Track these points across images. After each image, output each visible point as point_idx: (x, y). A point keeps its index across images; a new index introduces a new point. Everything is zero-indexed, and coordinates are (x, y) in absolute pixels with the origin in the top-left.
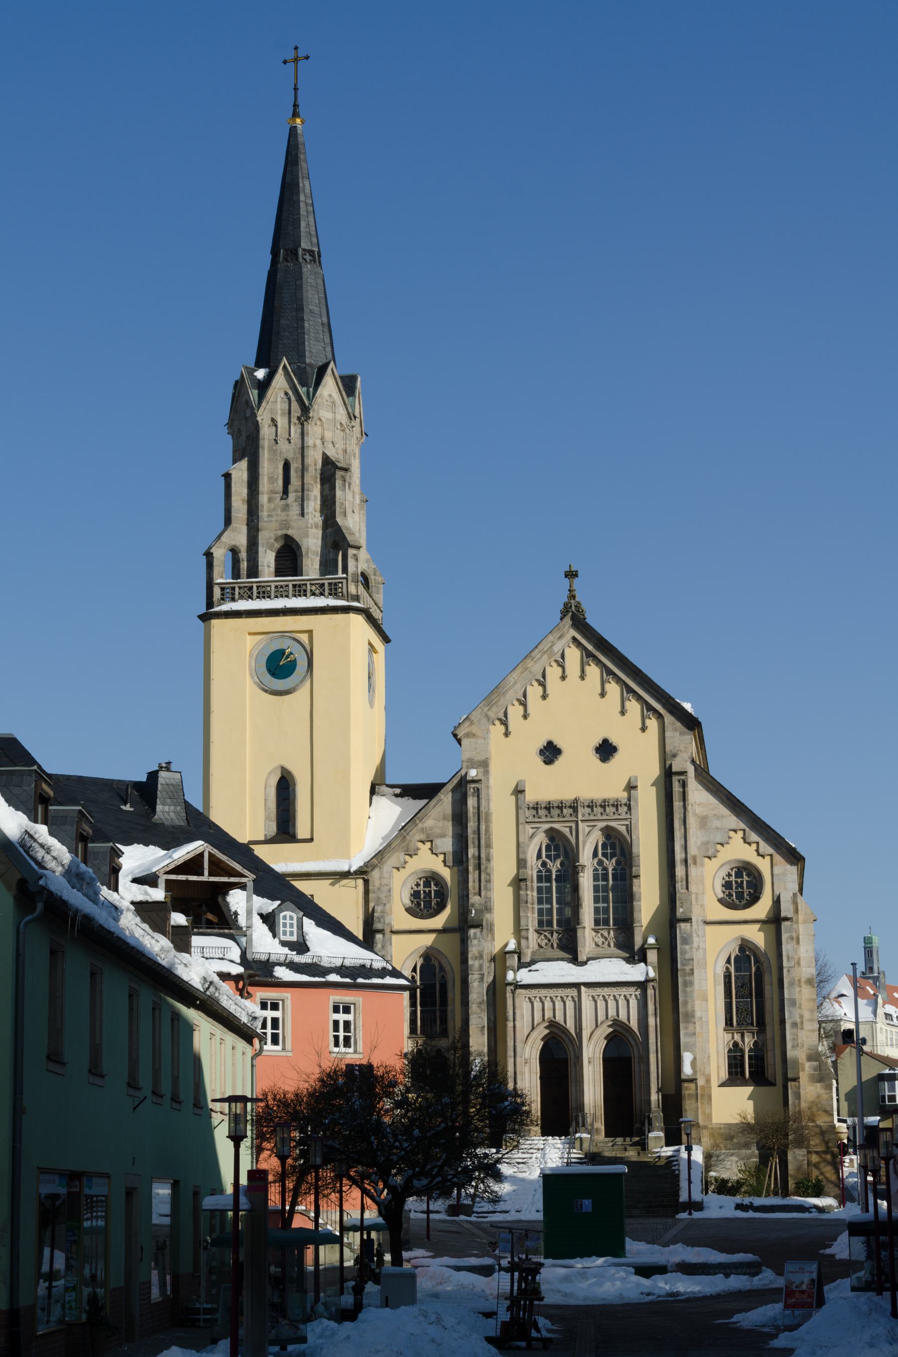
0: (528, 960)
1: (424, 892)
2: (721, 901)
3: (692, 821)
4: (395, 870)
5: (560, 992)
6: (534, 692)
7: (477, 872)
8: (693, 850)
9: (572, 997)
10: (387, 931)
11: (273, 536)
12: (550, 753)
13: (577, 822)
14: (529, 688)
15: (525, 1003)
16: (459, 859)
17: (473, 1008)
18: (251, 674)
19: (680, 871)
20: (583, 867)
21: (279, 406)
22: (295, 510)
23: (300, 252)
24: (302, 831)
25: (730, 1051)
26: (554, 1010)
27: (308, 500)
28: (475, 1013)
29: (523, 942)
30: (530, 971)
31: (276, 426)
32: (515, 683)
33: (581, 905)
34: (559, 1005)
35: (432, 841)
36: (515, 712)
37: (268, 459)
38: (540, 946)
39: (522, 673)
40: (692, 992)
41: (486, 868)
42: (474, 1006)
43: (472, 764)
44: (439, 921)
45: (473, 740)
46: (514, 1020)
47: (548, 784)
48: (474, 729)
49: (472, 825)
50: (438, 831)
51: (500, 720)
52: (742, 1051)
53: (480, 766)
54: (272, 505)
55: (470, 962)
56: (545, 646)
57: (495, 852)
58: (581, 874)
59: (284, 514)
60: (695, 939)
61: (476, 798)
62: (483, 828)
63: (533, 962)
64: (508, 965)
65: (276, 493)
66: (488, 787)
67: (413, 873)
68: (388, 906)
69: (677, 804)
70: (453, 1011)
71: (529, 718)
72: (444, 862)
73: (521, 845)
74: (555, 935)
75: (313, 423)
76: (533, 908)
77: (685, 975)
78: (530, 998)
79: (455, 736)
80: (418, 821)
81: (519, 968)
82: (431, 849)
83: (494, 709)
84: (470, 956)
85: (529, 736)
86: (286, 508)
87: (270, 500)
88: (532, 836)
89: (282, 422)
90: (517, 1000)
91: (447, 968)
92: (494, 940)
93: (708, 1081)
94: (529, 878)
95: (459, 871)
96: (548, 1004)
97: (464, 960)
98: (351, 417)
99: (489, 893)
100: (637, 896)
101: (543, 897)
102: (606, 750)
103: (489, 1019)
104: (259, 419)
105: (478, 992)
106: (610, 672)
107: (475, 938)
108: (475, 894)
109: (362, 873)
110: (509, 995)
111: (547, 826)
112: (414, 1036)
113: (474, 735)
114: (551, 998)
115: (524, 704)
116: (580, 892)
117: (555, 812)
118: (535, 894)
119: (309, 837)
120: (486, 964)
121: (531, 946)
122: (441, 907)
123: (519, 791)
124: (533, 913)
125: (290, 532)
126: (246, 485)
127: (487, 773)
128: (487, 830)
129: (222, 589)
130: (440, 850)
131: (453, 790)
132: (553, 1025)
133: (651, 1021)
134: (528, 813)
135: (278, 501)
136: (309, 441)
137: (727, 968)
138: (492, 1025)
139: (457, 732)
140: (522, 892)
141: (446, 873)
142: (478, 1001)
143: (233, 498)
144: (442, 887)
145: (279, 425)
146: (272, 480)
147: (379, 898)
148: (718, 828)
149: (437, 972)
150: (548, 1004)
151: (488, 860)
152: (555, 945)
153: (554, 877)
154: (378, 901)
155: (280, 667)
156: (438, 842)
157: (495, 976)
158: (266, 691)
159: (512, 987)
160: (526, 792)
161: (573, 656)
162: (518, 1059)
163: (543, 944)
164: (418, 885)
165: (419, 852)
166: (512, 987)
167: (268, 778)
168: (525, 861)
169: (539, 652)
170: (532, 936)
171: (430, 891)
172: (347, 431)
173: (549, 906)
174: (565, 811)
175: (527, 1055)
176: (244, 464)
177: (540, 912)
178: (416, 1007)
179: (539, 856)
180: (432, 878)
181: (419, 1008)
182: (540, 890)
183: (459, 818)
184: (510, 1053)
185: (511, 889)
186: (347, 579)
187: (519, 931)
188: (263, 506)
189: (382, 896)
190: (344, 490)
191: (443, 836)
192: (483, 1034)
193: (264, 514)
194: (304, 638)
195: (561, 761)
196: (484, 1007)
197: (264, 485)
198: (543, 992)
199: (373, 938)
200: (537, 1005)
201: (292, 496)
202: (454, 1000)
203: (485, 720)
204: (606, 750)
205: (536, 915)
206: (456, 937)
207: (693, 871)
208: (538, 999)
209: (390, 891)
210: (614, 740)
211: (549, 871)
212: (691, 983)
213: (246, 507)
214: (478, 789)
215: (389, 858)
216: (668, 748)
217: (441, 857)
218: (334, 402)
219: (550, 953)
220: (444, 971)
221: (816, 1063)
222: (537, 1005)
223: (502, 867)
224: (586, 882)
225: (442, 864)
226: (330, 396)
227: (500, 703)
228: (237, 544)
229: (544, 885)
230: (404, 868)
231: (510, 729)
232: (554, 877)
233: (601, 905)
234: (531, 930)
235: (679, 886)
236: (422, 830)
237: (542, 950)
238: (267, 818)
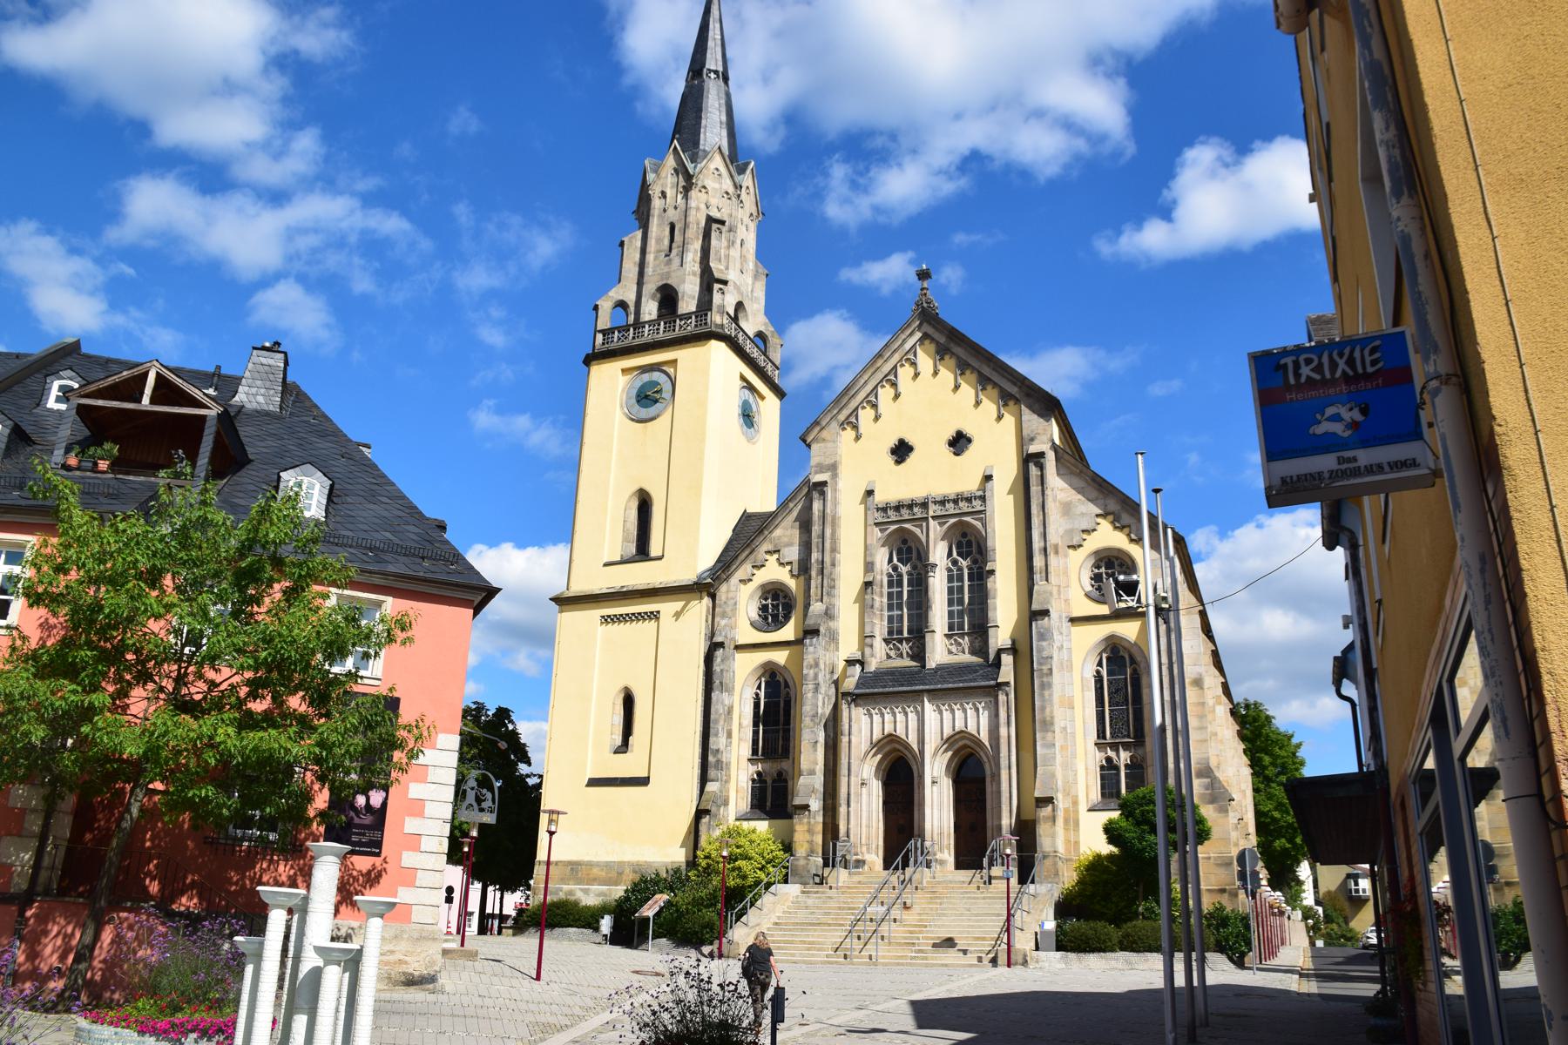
2: (1087, 595)
3: (1050, 505)
8: (1053, 538)
10: (729, 646)
12: (902, 451)
19: (1038, 561)
22: (677, 261)
24: (654, 550)
25: (1102, 768)
29: (868, 651)
38: (889, 657)
40: (1051, 695)
43: (821, 468)
47: (899, 485)
49: (816, 529)
50: (786, 540)
52: (1117, 768)
60: (1056, 636)
66: (835, 490)
69: (1035, 489)
77: (1041, 676)
85: (879, 434)
86: (669, 263)
89: (670, 193)
93: (1075, 803)
98: (738, 187)
100: (991, 594)
101: (894, 601)
102: (959, 442)
123: (870, 493)
127: (835, 476)
132: (891, 739)
133: (1003, 731)
136: (693, 204)
137: (1098, 672)
141: (792, 584)
146: (659, 240)
148: (1083, 514)
151: (833, 565)
155: (648, 399)
156: (785, 551)
170: (879, 644)
177: (890, 619)
182: (890, 595)
190: (720, 239)
191: (790, 544)
193: (649, 271)
195: (912, 459)
197: (652, 245)
204: (959, 442)
207: (1052, 559)
210: (968, 430)
212: (1050, 685)
216: (1025, 433)
221: (1207, 780)
223: (849, 574)
233: (955, 608)
235: (1037, 577)
238: (625, 540)
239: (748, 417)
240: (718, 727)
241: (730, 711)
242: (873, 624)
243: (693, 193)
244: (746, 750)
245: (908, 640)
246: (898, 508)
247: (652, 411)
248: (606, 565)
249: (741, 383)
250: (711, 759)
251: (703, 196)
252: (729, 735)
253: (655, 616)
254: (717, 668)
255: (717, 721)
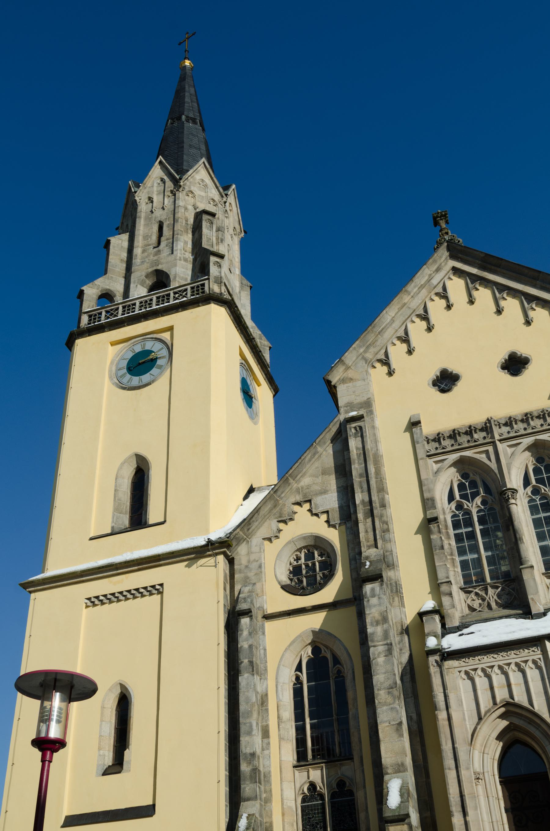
0: (456, 623)
1: (307, 566)
4: (267, 543)
5: (513, 657)
6: (417, 329)
7: (369, 520)
9: (534, 662)
11: (144, 274)
13: (494, 444)
14: (410, 326)
15: (460, 682)
16: (347, 516)
17: (381, 696)
18: (111, 378)
20: (514, 491)
21: (155, 189)
23: (184, 117)
24: (154, 513)
26: (509, 685)
27: (177, 241)
28: (385, 704)
29: (446, 600)
30: (460, 635)
31: (152, 202)
32: (393, 320)
33: (521, 539)
34: (515, 677)
35: (310, 501)
36: (397, 352)
37: (145, 225)
38: (472, 609)
39: (400, 309)
41: (381, 516)
42: (382, 692)
44: (328, 594)
45: (350, 384)
46: (447, 708)
48: (350, 374)
49: (356, 468)
50: (317, 488)
51: (379, 361)
53: (361, 408)
54: (146, 254)
55: (370, 630)
56: (422, 277)
57: (392, 498)
58: (512, 501)
59: (156, 258)
61: (360, 439)
62: (372, 470)
63: (464, 625)
64: (426, 631)
65: (149, 245)
66: (373, 427)
67: (289, 543)
68: (258, 586)
70: (356, 717)
71: (414, 353)
72: (328, 522)
73: (425, 482)
74: (490, 591)
75: (184, 192)
76: (453, 560)
78: (467, 673)
79: (328, 382)
80: (291, 480)
81: (443, 636)
82: (310, 510)
83: (372, 350)
84: (368, 620)
87: (144, 251)
88: (437, 472)
90: (447, 678)
91: (343, 657)
92: (403, 605)
94: (441, 517)
95: (347, 528)
96: (498, 679)
97: (364, 639)
99: (388, 546)
101: (466, 542)
103: (409, 718)
104: (137, 198)
105: (387, 670)
106: (502, 288)
107: (373, 596)
108: (369, 547)
109: (222, 547)
110: (434, 670)
111: (454, 457)
112: (302, 763)
113: (351, 379)
114: (500, 667)
115: (405, 339)
116: (516, 523)
117: (463, 439)
118: (453, 543)
119: (163, 520)
120: (395, 638)
121: (458, 607)
122: (328, 578)
123: (414, 424)
124: (454, 565)
125: (160, 267)
126: (126, 251)
127: (371, 412)
128: (378, 472)
129: (90, 316)
130: (321, 509)
131: (333, 440)
132: (511, 710)
134: (427, 447)
135: (151, 250)
136: (180, 203)
138: (415, 727)
139: (330, 378)
140: (434, 537)
141: (333, 536)
142: (387, 684)
143: (110, 257)
144: (329, 556)
145: (155, 200)
147: (247, 578)
149: (331, 664)
150: (498, 679)
151: (383, 505)
152: (493, 605)
153: (476, 519)
154: (246, 581)
155: (140, 365)
157: (411, 656)
158: (124, 388)
159: (437, 657)
160: (422, 424)
161: (457, 287)
162: (464, 773)
163: (476, 604)
164: (298, 559)
165: (296, 517)
166: (437, 657)
167: (120, 468)
168: (433, 500)
169: (415, 287)
170: (459, 596)
171: (314, 564)
172: (220, 205)
173: (476, 556)
174: (476, 436)
175: (477, 766)
176: (125, 237)
177: (464, 565)
178: (304, 720)
179: (451, 497)
180: (316, 546)
181: (308, 720)
182: (459, 538)
183: (343, 469)
184: (449, 762)
185: (419, 537)
186: (208, 279)
187: (437, 587)
188: (136, 255)
189: (251, 574)
191: (324, 492)
192: (401, 735)
193: (137, 261)
194: (166, 336)
196: (398, 692)
197: (139, 241)
198: (487, 660)
199: (237, 623)
200: (481, 682)
201: (163, 244)
202: (355, 699)
203: (362, 363)
205: (459, 569)
206: (352, 611)
208: (479, 672)
209: (260, 567)
210: (523, 350)
211: (468, 513)
213: (125, 265)
214: (361, 428)
215: (258, 528)
217: (324, 517)
218: (206, 186)
219: (487, 614)
220: (340, 664)
222: (481, 682)
223: (403, 512)
224: (521, 512)
225: (326, 525)
226: (203, 180)
227: (378, 343)
228: (112, 289)
229: (463, 530)
230: (277, 537)
231: (393, 366)
232: (476, 519)
234: (455, 589)
236: (298, 491)
237: (474, 613)
238: (117, 509)
239: (248, 397)
240: (250, 721)
241: (264, 700)
242: (447, 570)
243: (181, 195)
244: (289, 754)
245: (495, 587)
246: (454, 435)
247: (146, 378)
248: (91, 539)
249: (238, 359)
250: (244, 767)
251: (190, 200)
252: (266, 733)
253: (157, 590)
254: (243, 643)
255: (249, 714)
